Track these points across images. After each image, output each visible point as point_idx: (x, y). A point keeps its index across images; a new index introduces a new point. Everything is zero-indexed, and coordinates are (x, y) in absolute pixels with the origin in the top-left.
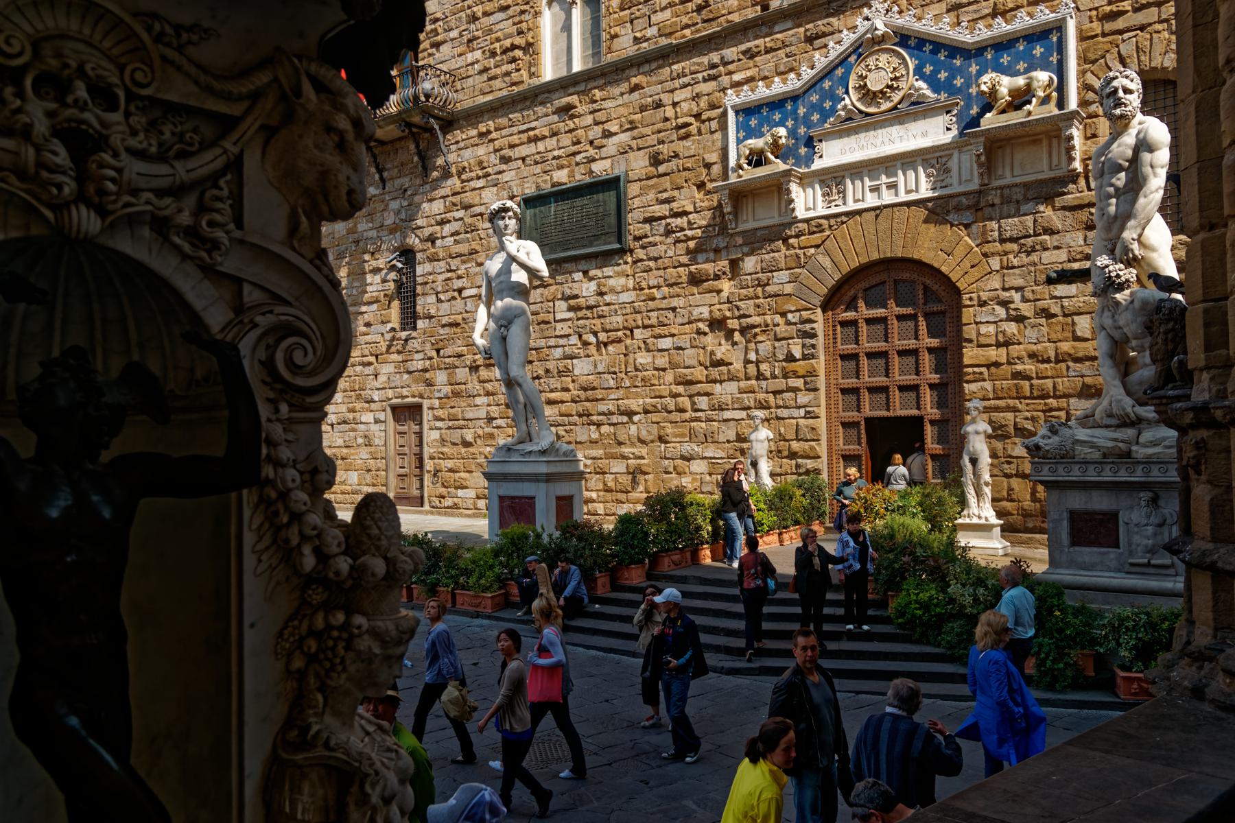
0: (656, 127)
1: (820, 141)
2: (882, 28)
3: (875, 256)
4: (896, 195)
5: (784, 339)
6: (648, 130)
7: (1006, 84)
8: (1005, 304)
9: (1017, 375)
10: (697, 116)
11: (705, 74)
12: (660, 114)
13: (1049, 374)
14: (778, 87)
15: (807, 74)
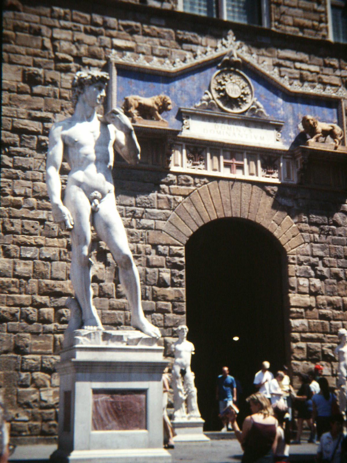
0: (31, 50)
1: (188, 117)
2: (235, 58)
3: (229, 214)
4: (244, 174)
5: (156, 266)
6: (22, 50)
7: (321, 126)
8: (313, 266)
9: (323, 317)
10: (78, 59)
11: (88, 27)
12: (37, 42)
13: (340, 317)
14: (155, 64)
15: (180, 66)
